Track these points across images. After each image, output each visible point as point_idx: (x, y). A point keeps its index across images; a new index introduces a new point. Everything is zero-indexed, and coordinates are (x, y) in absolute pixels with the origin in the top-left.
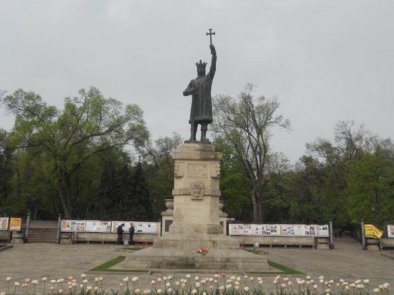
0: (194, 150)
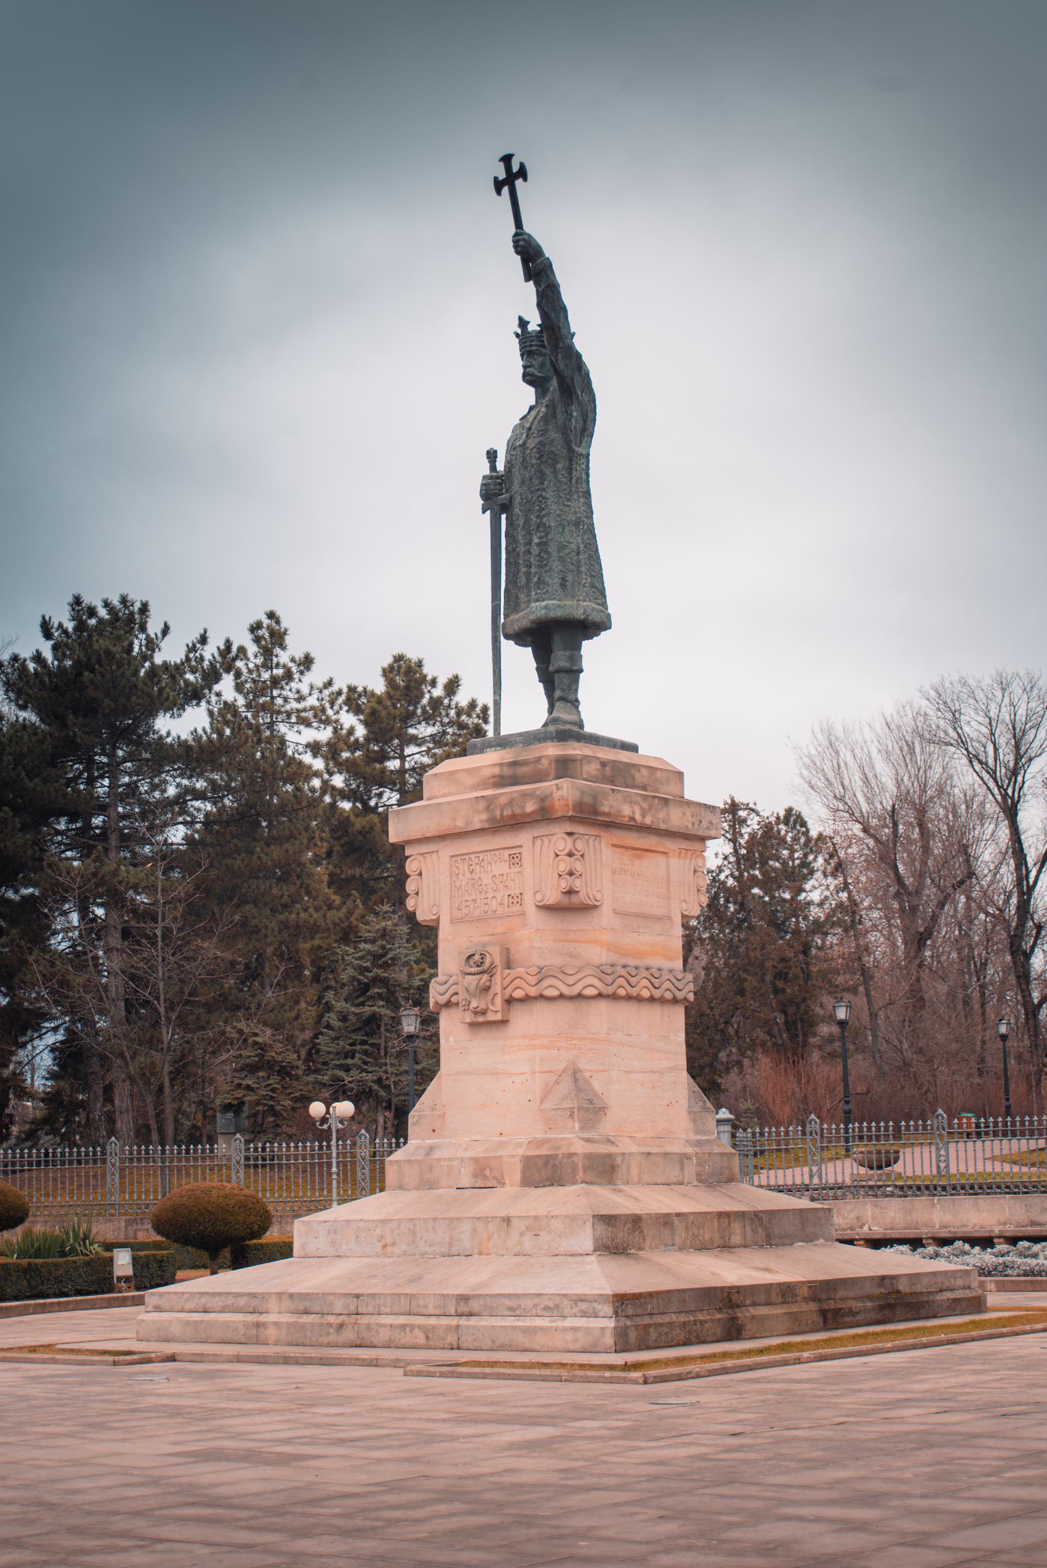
0: (475, 788)
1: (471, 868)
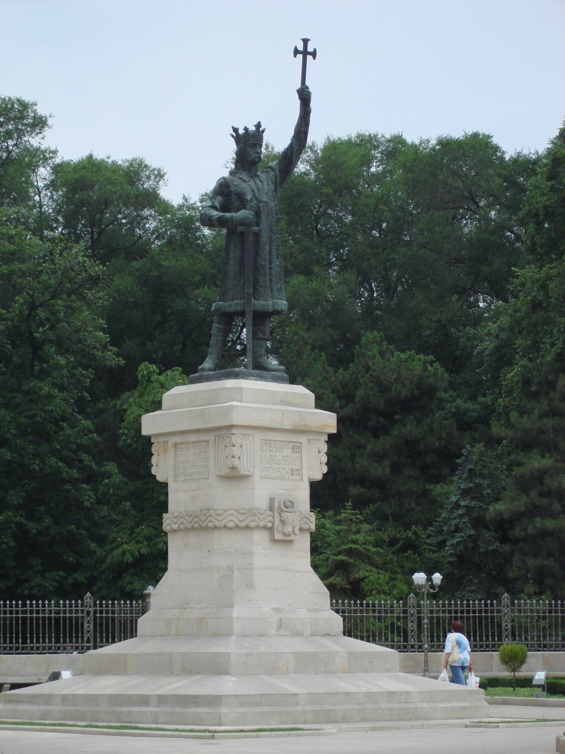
1: (271, 449)
